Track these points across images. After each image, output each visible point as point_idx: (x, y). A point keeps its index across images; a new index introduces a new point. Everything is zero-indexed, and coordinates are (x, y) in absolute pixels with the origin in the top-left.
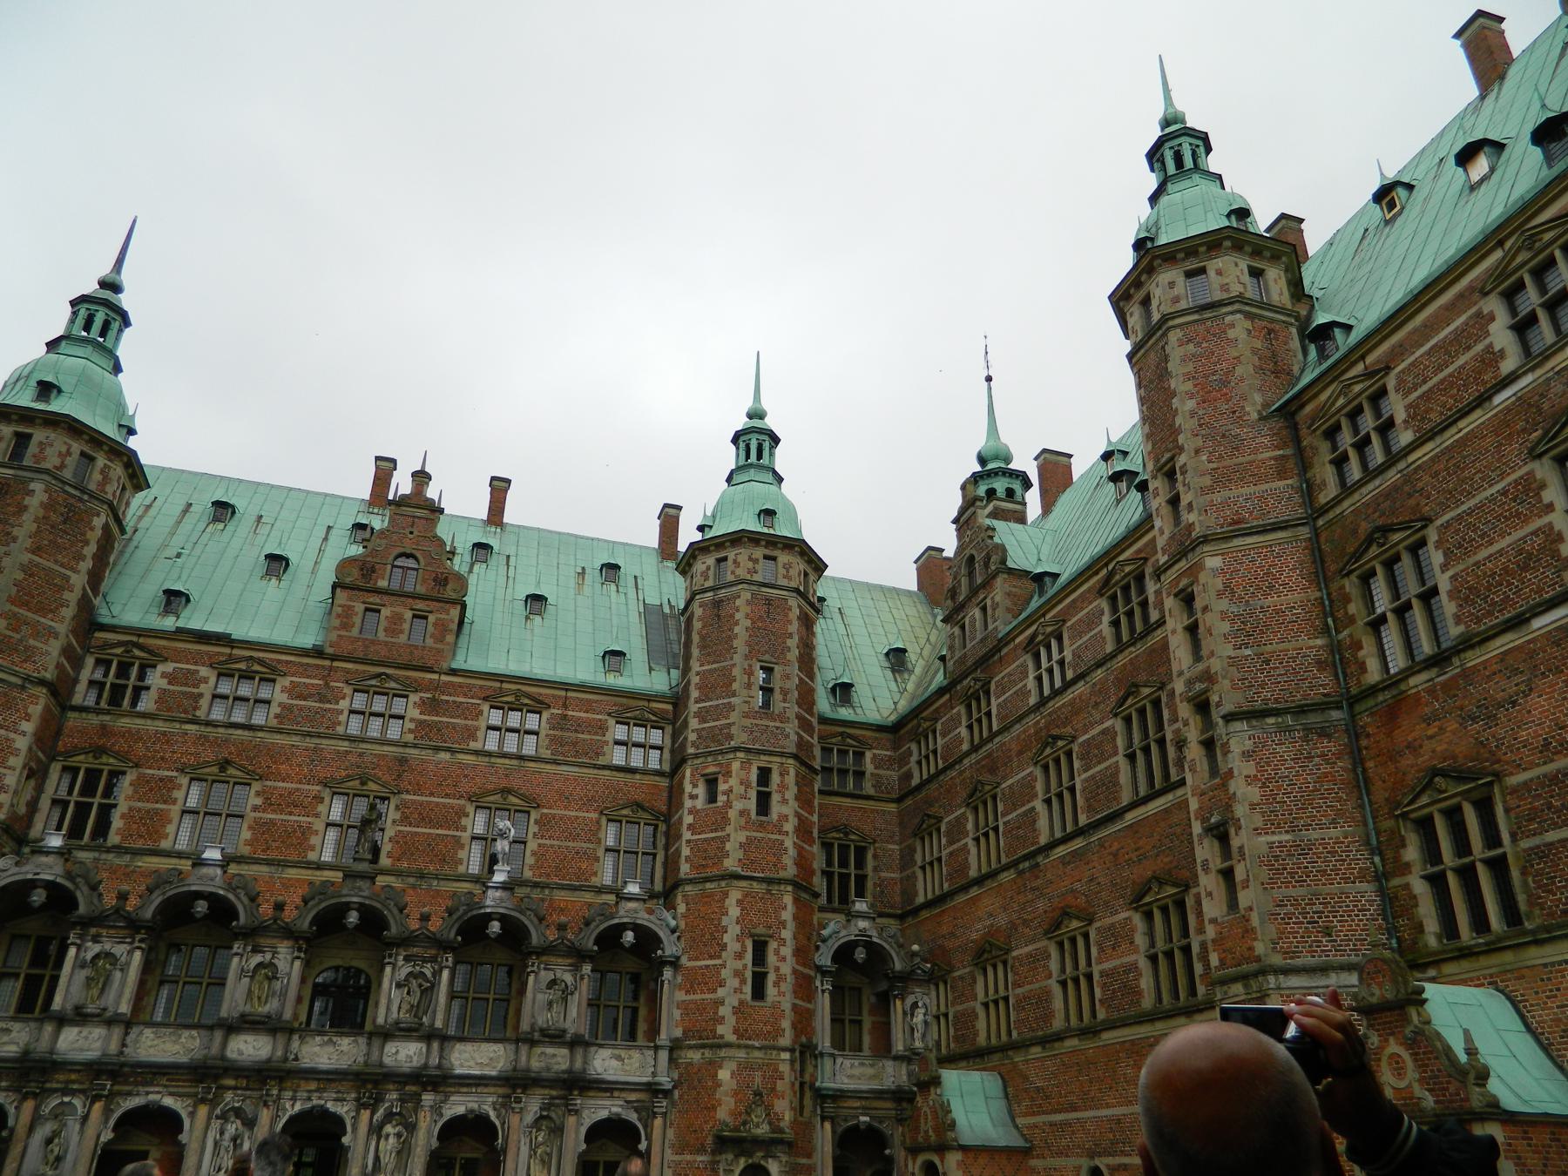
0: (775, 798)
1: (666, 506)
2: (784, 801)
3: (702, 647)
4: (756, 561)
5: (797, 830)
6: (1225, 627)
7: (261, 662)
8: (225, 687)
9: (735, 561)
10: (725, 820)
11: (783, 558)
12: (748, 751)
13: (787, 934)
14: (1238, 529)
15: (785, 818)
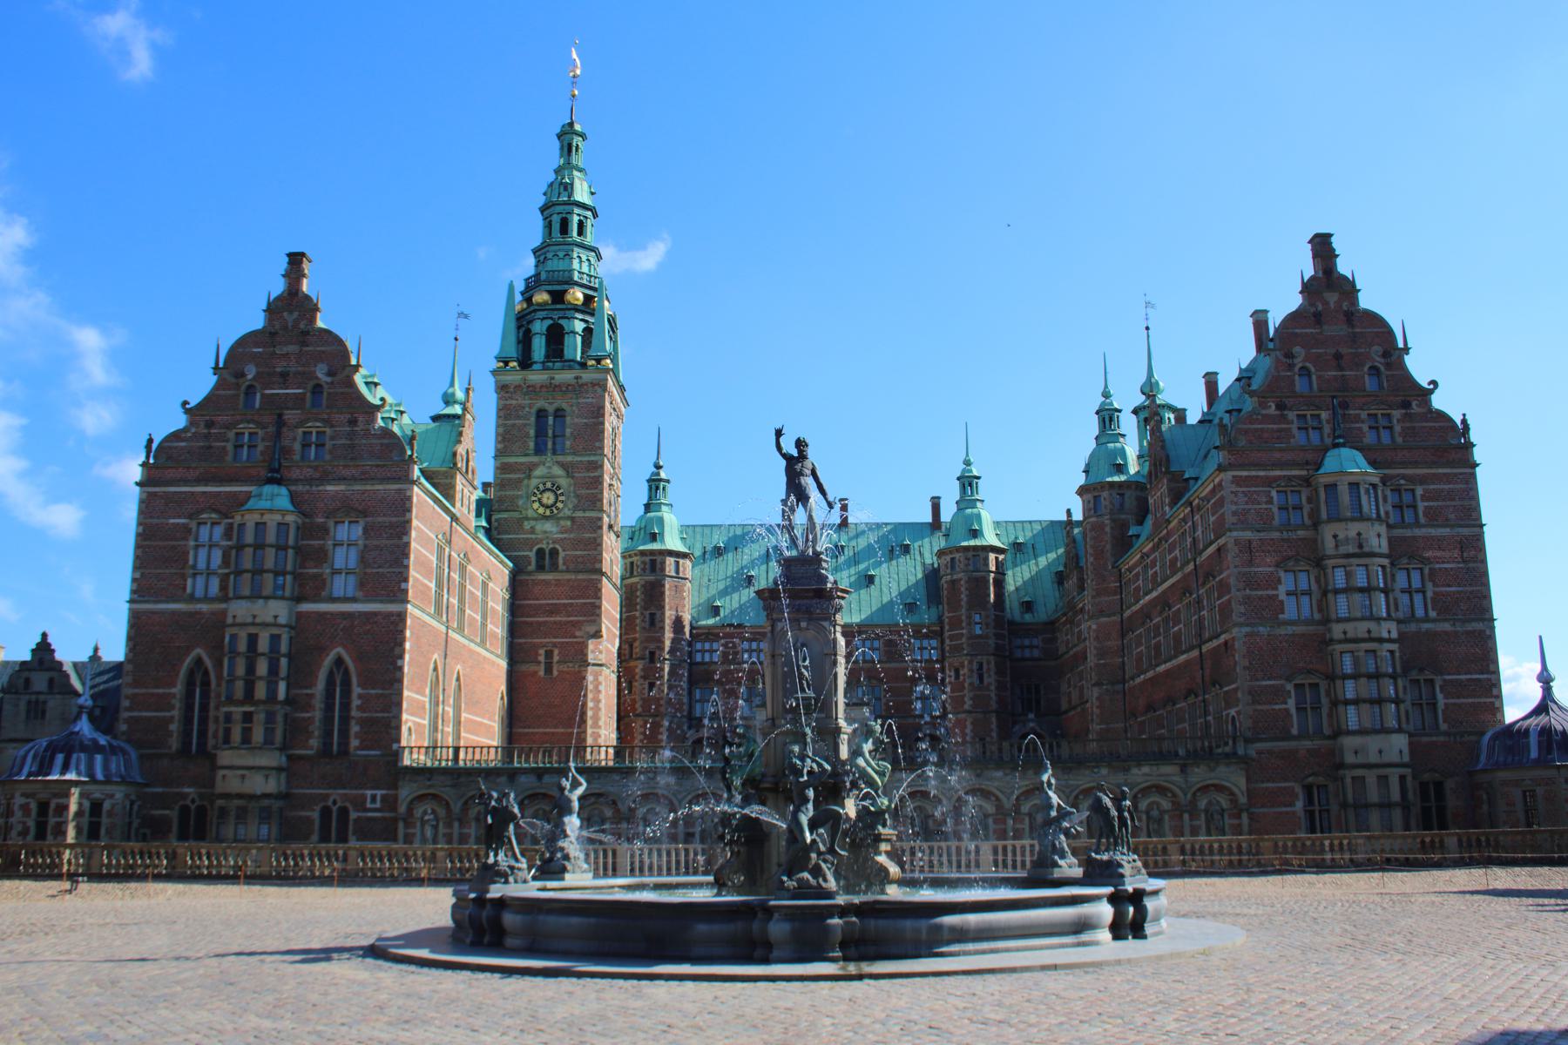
0: (985, 675)
1: (933, 498)
2: (990, 676)
3: (948, 604)
4: (969, 559)
5: (997, 688)
6: (1095, 652)
7: (759, 633)
8: (746, 645)
9: (960, 561)
10: (964, 688)
11: (982, 555)
12: (972, 655)
13: (994, 734)
14: (1101, 613)
15: (989, 684)
